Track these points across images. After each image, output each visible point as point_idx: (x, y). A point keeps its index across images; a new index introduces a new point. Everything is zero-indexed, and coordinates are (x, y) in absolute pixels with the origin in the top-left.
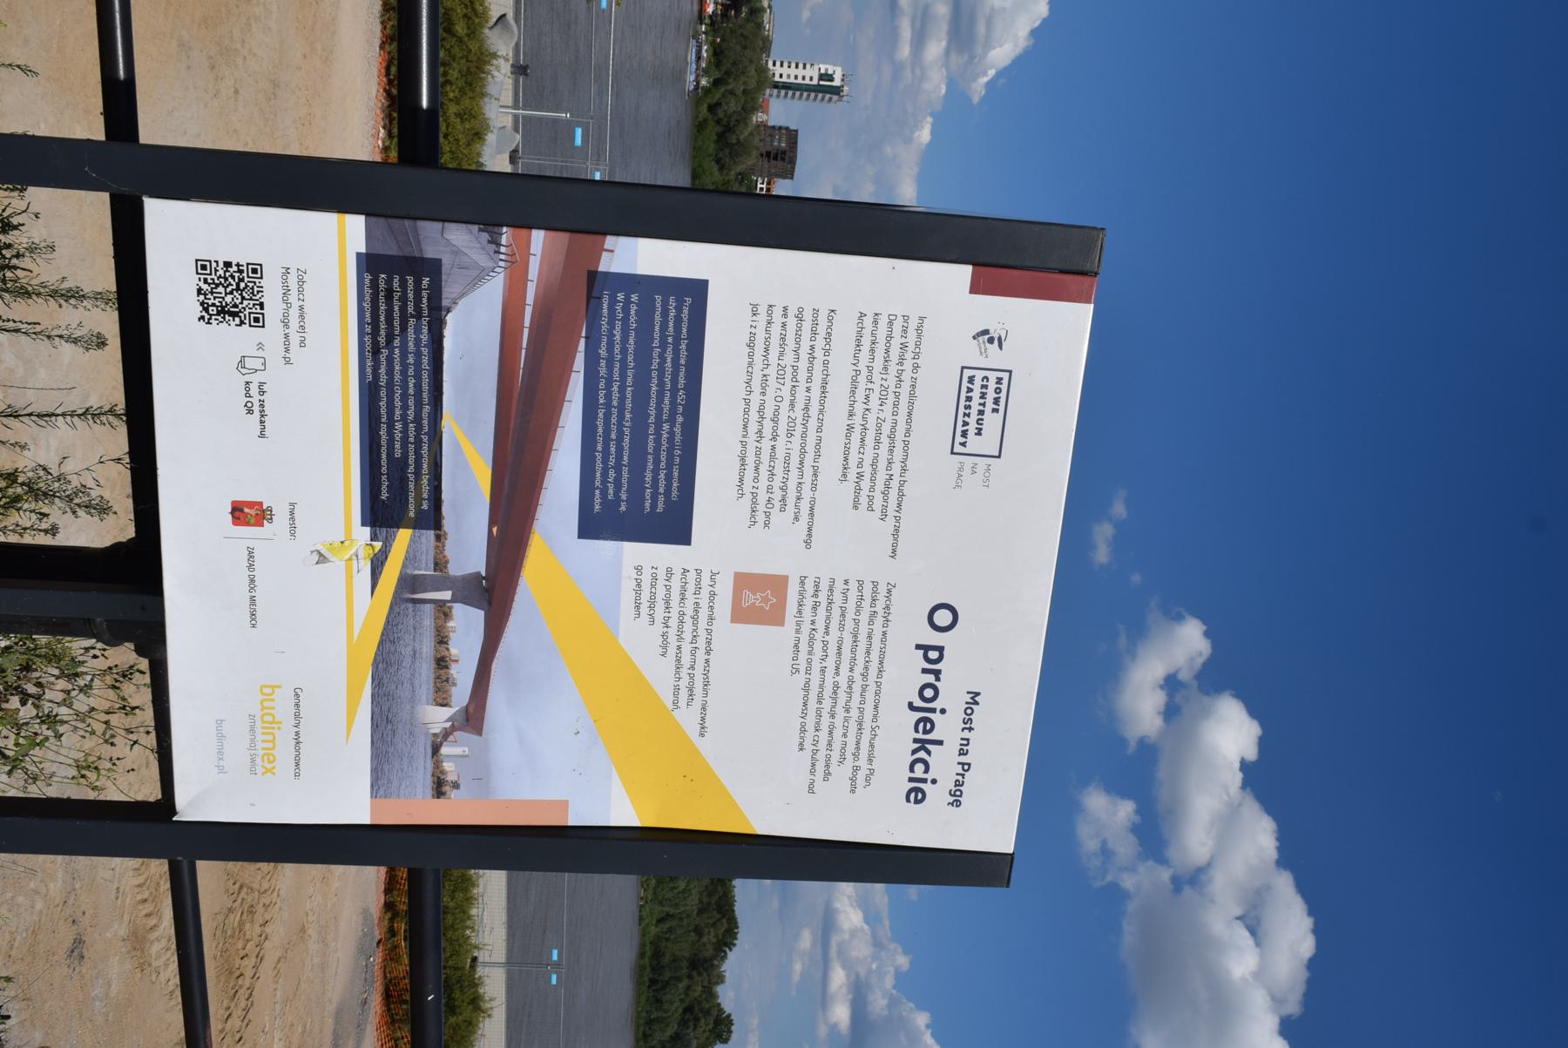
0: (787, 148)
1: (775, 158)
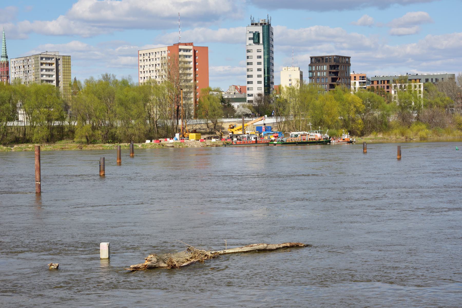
0: (328, 64)
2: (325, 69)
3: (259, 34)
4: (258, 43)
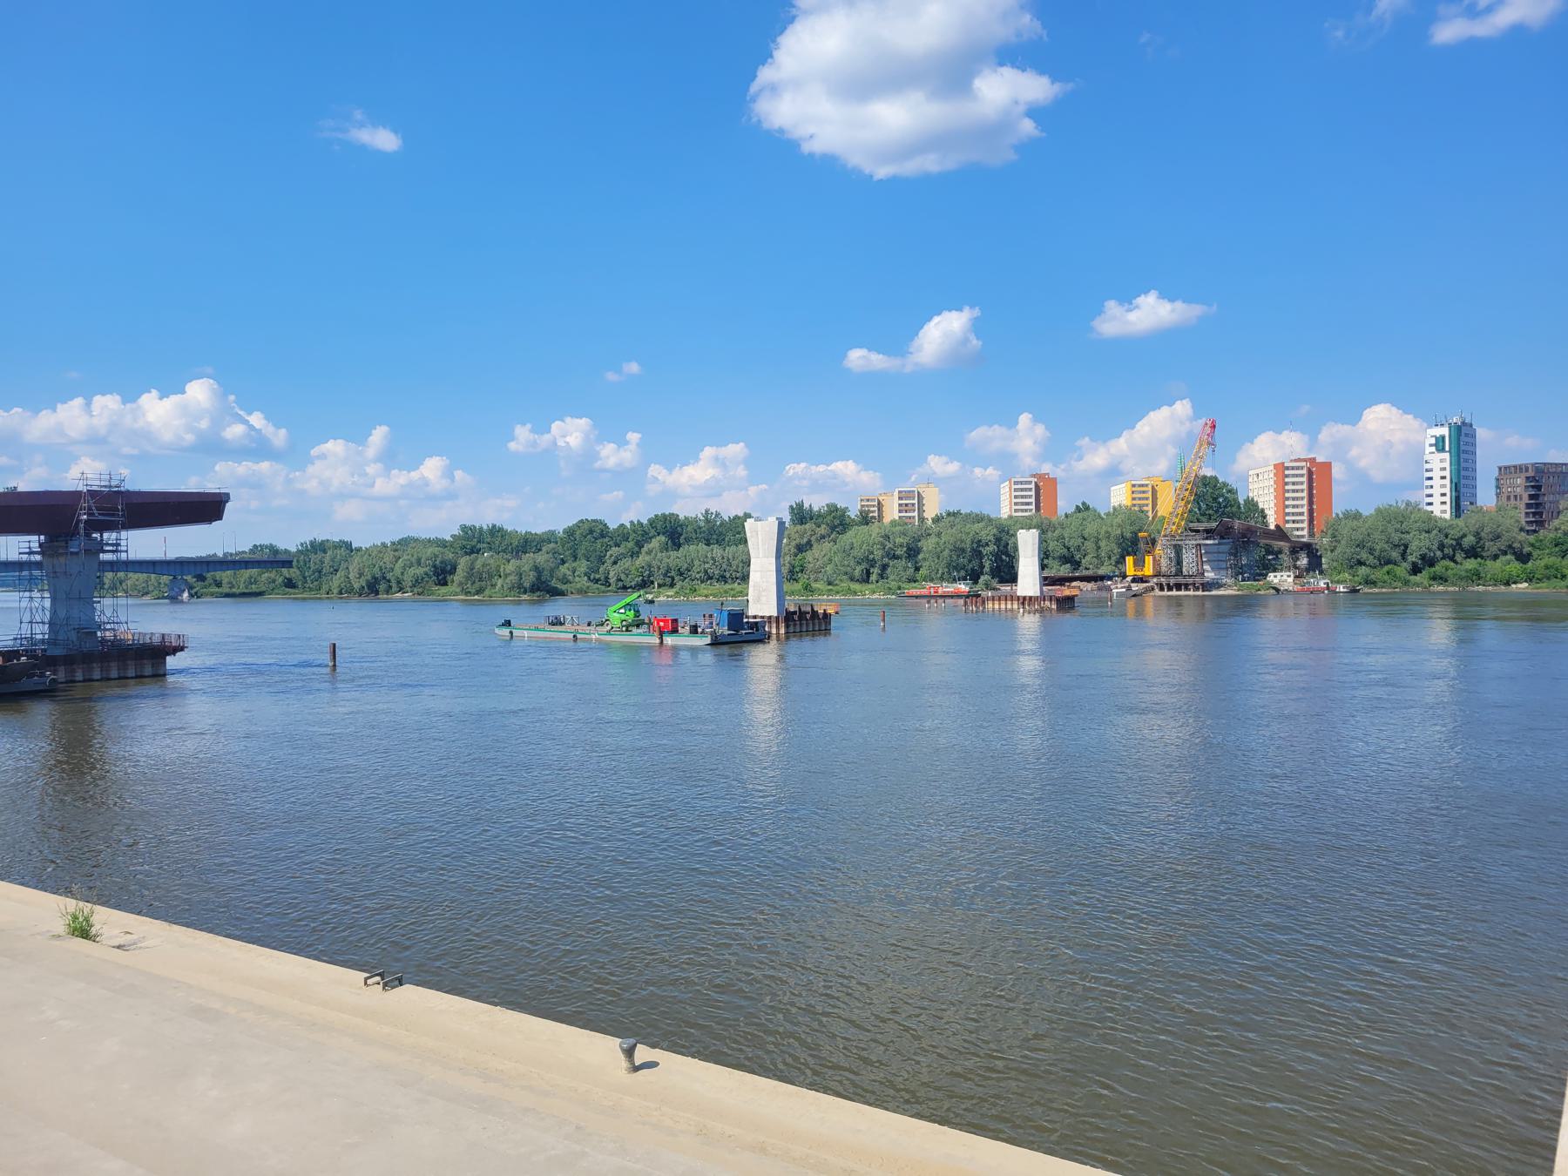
1: (1539, 488)
3: (1443, 438)
4: (1443, 450)
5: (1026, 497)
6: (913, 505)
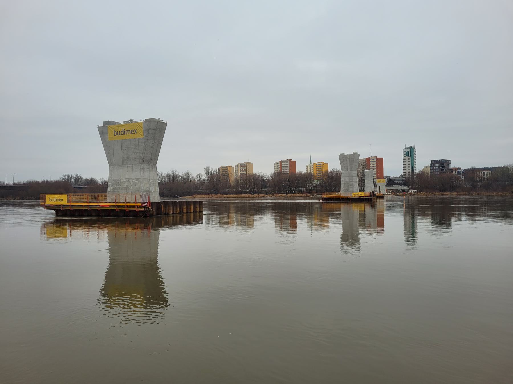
2: (438, 165)
3: (409, 152)
5: (286, 167)
6: (245, 169)
